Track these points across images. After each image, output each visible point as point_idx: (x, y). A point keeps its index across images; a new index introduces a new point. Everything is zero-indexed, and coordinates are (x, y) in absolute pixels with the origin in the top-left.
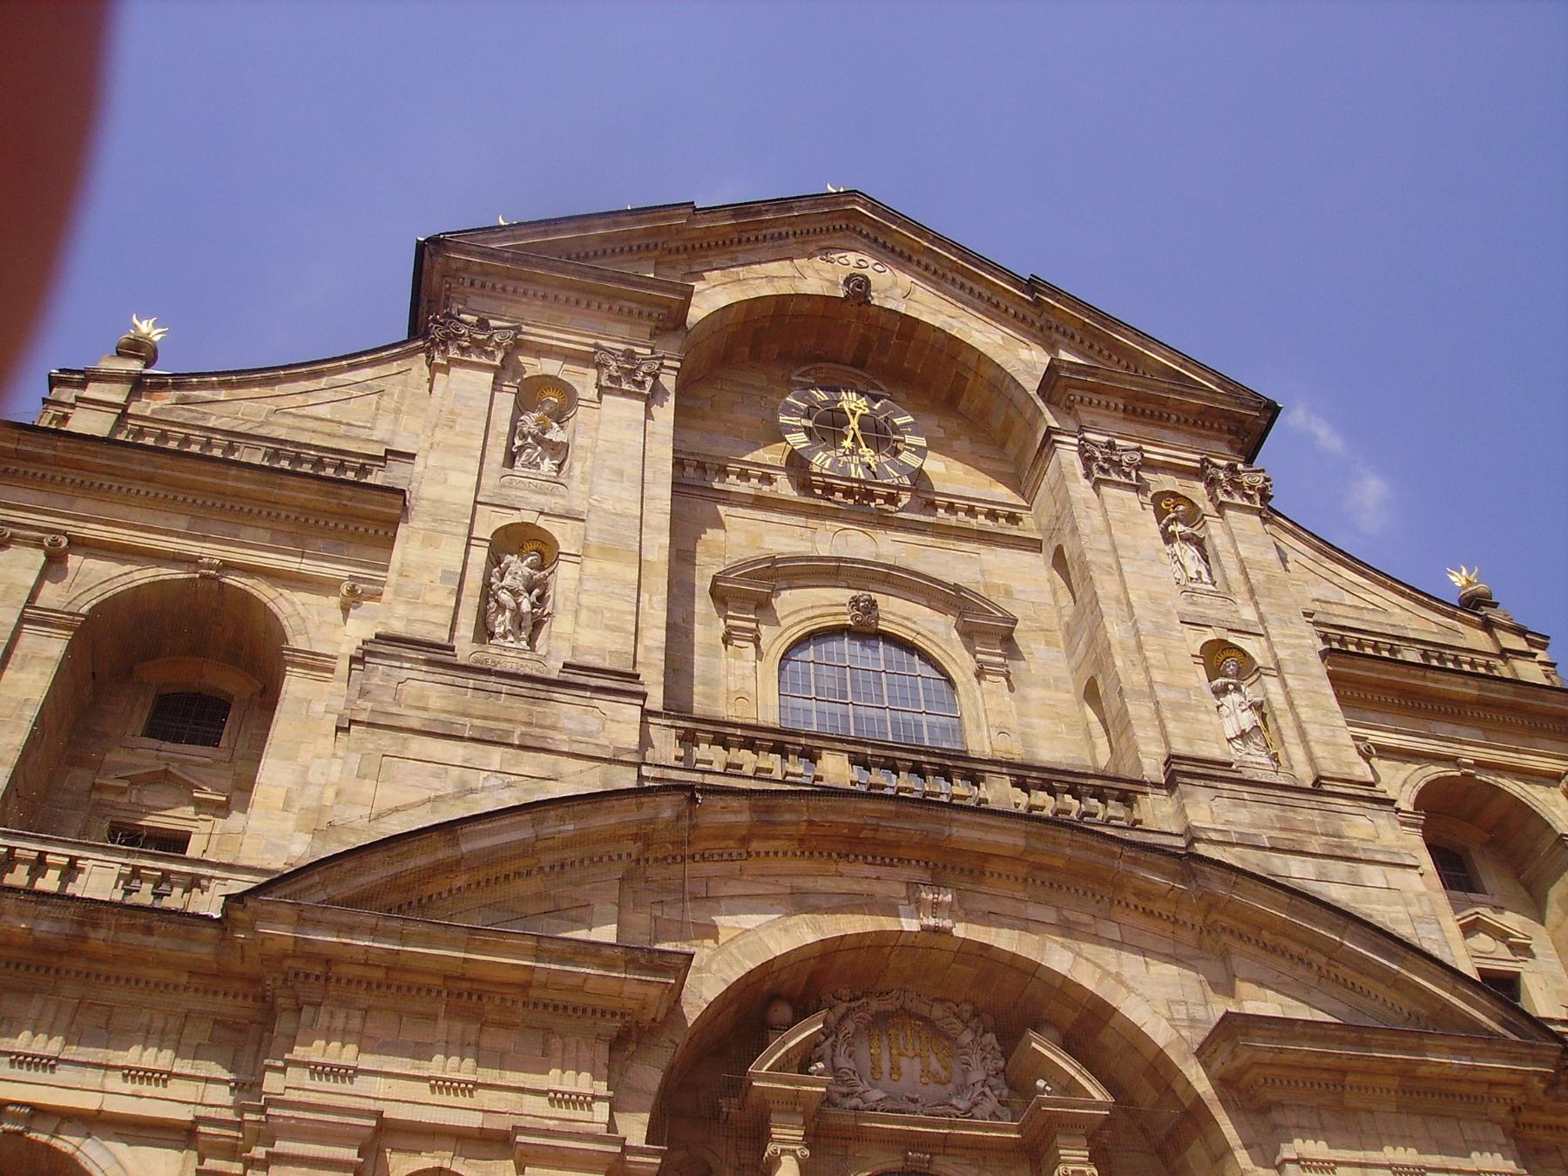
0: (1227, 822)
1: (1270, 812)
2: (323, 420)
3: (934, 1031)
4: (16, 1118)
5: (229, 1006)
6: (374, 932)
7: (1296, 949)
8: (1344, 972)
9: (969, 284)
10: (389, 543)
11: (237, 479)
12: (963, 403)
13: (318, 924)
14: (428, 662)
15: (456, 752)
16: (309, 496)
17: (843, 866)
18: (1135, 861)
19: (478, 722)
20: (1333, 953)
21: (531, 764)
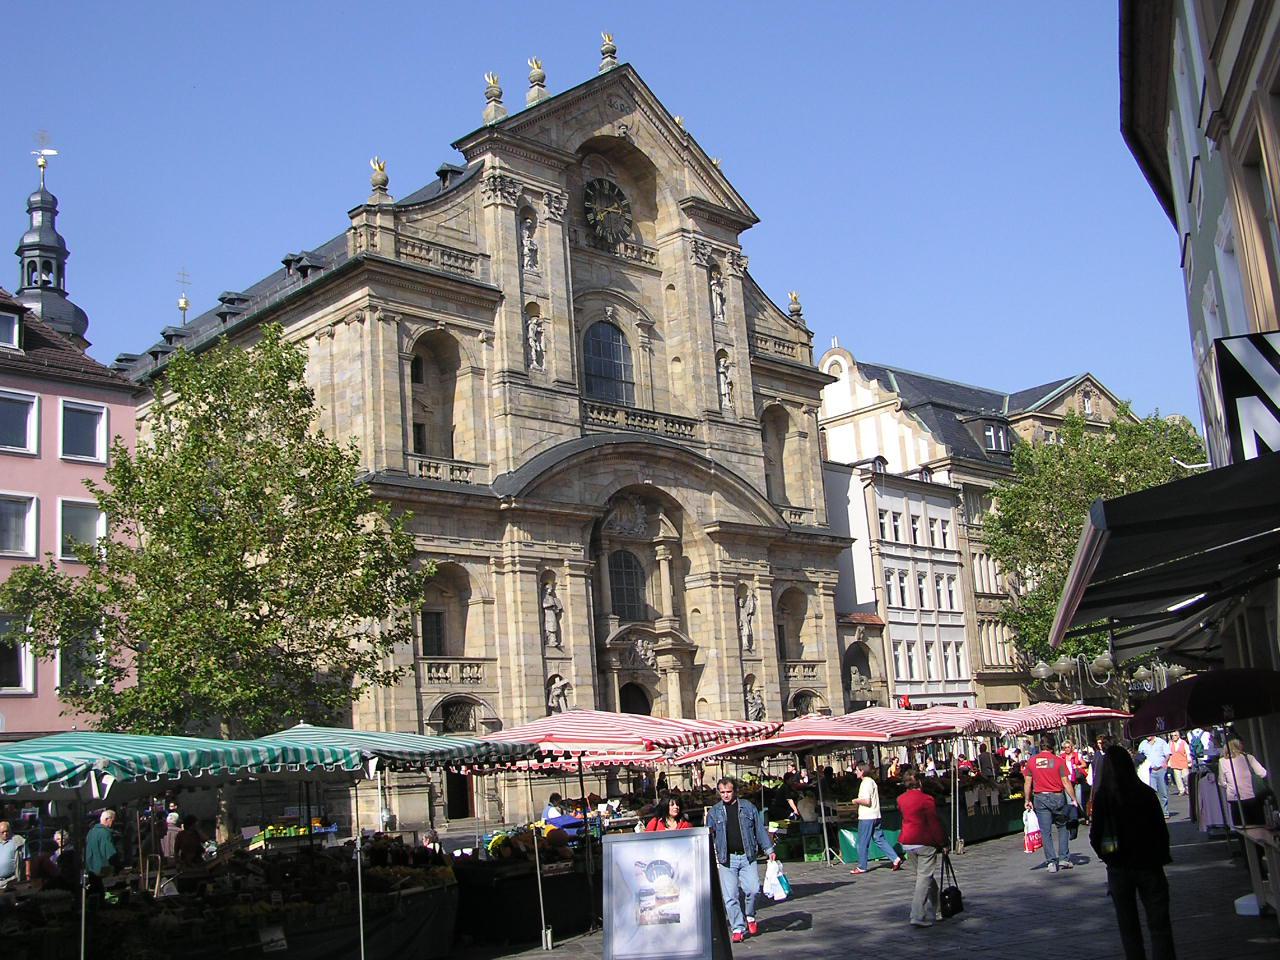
0: (719, 440)
1: (730, 435)
2: (453, 229)
3: (632, 505)
4: (452, 558)
5: (491, 519)
6: (540, 504)
7: (731, 491)
8: (743, 500)
9: (660, 127)
10: (493, 311)
11: (451, 285)
12: (641, 183)
13: (529, 503)
14: (525, 385)
15: (535, 424)
16: (471, 292)
17: (626, 461)
18: (700, 463)
19: (542, 411)
20: (741, 494)
21: (556, 428)
